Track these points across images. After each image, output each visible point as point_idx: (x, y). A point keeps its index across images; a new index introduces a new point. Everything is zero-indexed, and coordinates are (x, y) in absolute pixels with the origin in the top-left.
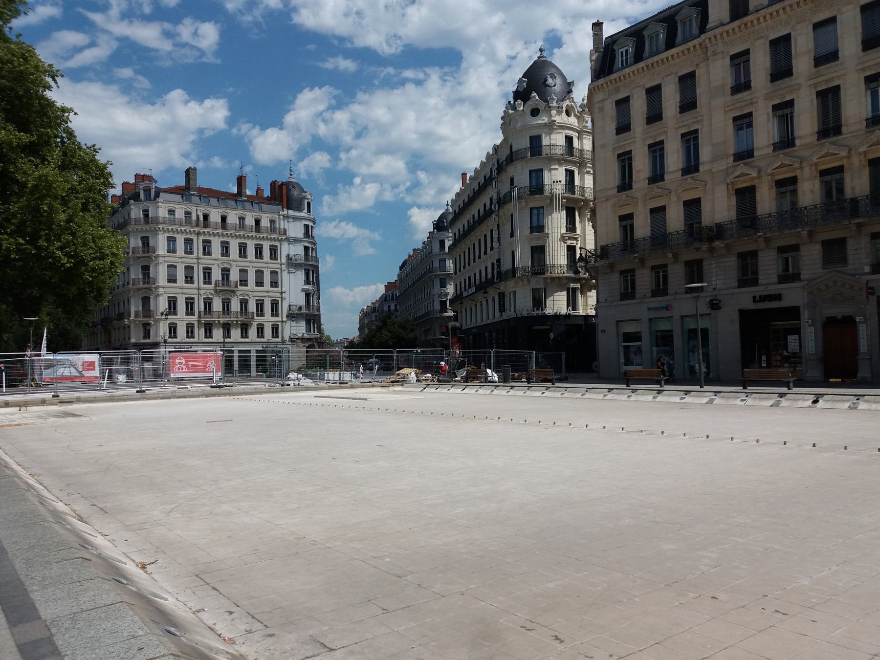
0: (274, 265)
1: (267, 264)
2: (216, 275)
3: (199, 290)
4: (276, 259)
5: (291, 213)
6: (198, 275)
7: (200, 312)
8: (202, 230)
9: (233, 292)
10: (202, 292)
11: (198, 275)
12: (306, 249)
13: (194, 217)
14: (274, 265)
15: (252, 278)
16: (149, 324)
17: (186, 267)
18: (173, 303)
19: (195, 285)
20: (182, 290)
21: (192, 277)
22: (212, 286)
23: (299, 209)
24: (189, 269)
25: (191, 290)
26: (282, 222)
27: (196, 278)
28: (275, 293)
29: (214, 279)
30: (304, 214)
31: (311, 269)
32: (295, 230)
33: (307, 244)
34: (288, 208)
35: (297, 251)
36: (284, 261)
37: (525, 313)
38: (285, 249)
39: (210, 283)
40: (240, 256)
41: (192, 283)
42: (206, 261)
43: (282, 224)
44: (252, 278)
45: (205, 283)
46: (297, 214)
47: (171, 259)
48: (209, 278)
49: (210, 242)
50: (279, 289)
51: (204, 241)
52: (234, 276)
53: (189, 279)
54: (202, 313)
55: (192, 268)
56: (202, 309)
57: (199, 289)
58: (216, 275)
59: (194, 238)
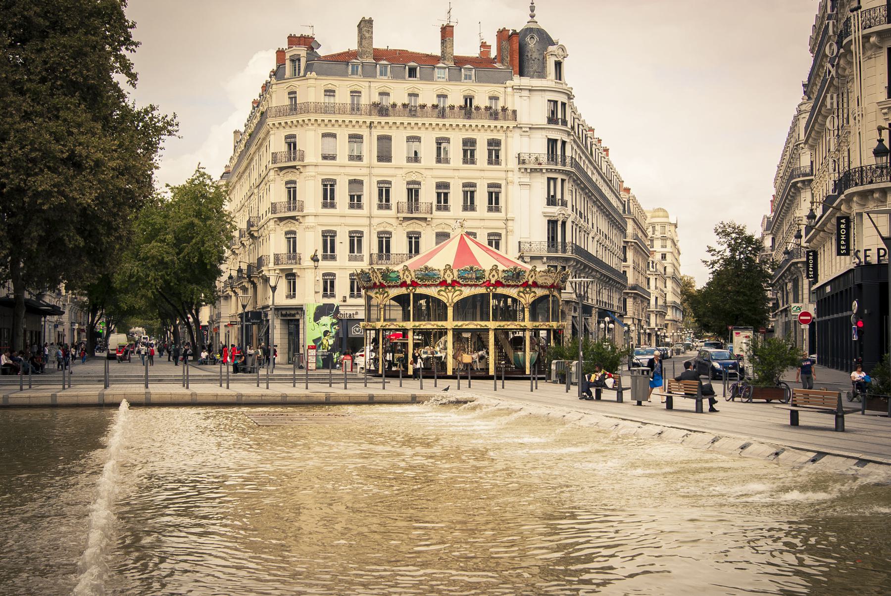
0: (494, 174)
1: (482, 174)
2: (399, 195)
3: (371, 219)
4: (497, 162)
5: (526, 81)
6: (370, 195)
7: (371, 255)
8: (376, 119)
9: (425, 219)
10: (375, 221)
11: (370, 195)
12: (552, 142)
13: (364, 101)
14: (494, 174)
15: (456, 197)
16: (294, 275)
17: (351, 182)
18: (329, 240)
19: (364, 212)
20: (343, 219)
21: (359, 197)
22: (393, 212)
23: (541, 74)
24: (356, 183)
25: (357, 220)
26: (509, 99)
27: (365, 200)
28: (494, 221)
29: (393, 201)
30: (550, 81)
31: (560, 177)
32: (533, 110)
33: (553, 136)
34: (521, 74)
35: (538, 146)
36: (513, 164)
37: (874, 260)
38: (516, 145)
39: (388, 207)
40: (465, 161)
41: (359, 207)
42: (383, 171)
43: (513, 101)
44: (456, 197)
45: (380, 207)
46: (536, 83)
47: (328, 170)
48: (388, 200)
49: (388, 138)
50: (502, 215)
51: (380, 138)
52: (428, 195)
53: (356, 201)
54: (375, 257)
55: (361, 183)
56: (375, 250)
57: (370, 217)
58: (399, 195)
59: (364, 132)
